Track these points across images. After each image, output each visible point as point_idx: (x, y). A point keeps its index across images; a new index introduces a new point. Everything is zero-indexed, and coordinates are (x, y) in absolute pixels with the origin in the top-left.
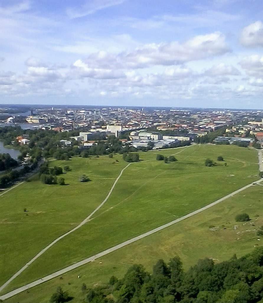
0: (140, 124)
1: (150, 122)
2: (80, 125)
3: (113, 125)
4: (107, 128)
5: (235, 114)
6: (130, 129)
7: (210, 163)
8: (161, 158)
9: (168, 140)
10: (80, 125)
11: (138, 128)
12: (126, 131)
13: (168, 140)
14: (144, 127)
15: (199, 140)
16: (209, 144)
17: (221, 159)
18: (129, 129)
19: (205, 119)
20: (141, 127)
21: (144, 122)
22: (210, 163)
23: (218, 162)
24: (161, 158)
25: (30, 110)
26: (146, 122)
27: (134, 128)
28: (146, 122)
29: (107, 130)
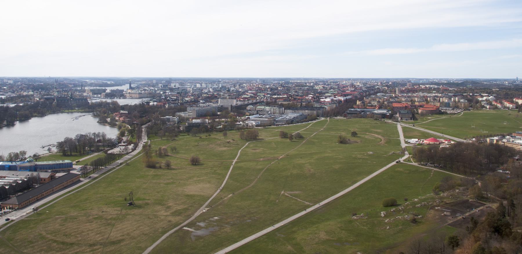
0: (256, 97)
1: (268, 94)
2: (187, 99)
3: (226, 98)
4: (219, 102)
5: (365, 84)
6: (246, 103)
7: (343, 141)
8: (284, 135)
9: (291, 115)
10: (187, 99)
11: (254, 101)
12: (241, 105)
13: (291, 115)
14: (262, 100)
15: (326, 114)
16: (339, 118)
17: (354, 134)
18: (244, 103)
19: (332, 90)
20: (258, 101)
21: (262, 95)
22: (343, 141)
23: (353, 139)
24: (284, 135)
25: (127, 83)
26: (263, 94)
27: (250, 102)
28: (263, 94)
29: (218, 104)
